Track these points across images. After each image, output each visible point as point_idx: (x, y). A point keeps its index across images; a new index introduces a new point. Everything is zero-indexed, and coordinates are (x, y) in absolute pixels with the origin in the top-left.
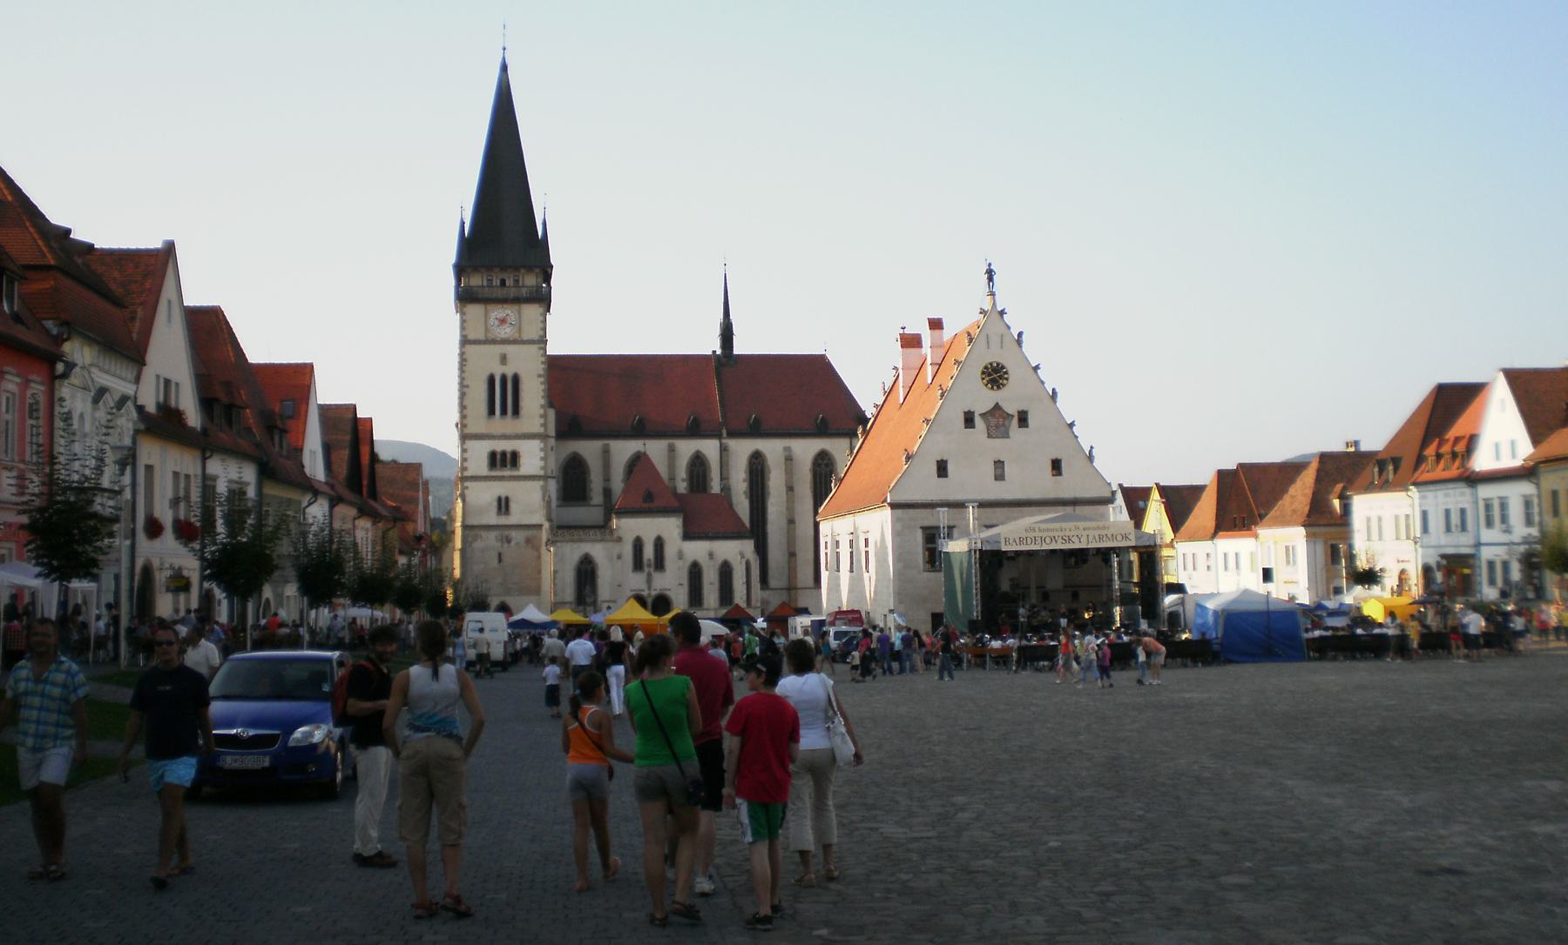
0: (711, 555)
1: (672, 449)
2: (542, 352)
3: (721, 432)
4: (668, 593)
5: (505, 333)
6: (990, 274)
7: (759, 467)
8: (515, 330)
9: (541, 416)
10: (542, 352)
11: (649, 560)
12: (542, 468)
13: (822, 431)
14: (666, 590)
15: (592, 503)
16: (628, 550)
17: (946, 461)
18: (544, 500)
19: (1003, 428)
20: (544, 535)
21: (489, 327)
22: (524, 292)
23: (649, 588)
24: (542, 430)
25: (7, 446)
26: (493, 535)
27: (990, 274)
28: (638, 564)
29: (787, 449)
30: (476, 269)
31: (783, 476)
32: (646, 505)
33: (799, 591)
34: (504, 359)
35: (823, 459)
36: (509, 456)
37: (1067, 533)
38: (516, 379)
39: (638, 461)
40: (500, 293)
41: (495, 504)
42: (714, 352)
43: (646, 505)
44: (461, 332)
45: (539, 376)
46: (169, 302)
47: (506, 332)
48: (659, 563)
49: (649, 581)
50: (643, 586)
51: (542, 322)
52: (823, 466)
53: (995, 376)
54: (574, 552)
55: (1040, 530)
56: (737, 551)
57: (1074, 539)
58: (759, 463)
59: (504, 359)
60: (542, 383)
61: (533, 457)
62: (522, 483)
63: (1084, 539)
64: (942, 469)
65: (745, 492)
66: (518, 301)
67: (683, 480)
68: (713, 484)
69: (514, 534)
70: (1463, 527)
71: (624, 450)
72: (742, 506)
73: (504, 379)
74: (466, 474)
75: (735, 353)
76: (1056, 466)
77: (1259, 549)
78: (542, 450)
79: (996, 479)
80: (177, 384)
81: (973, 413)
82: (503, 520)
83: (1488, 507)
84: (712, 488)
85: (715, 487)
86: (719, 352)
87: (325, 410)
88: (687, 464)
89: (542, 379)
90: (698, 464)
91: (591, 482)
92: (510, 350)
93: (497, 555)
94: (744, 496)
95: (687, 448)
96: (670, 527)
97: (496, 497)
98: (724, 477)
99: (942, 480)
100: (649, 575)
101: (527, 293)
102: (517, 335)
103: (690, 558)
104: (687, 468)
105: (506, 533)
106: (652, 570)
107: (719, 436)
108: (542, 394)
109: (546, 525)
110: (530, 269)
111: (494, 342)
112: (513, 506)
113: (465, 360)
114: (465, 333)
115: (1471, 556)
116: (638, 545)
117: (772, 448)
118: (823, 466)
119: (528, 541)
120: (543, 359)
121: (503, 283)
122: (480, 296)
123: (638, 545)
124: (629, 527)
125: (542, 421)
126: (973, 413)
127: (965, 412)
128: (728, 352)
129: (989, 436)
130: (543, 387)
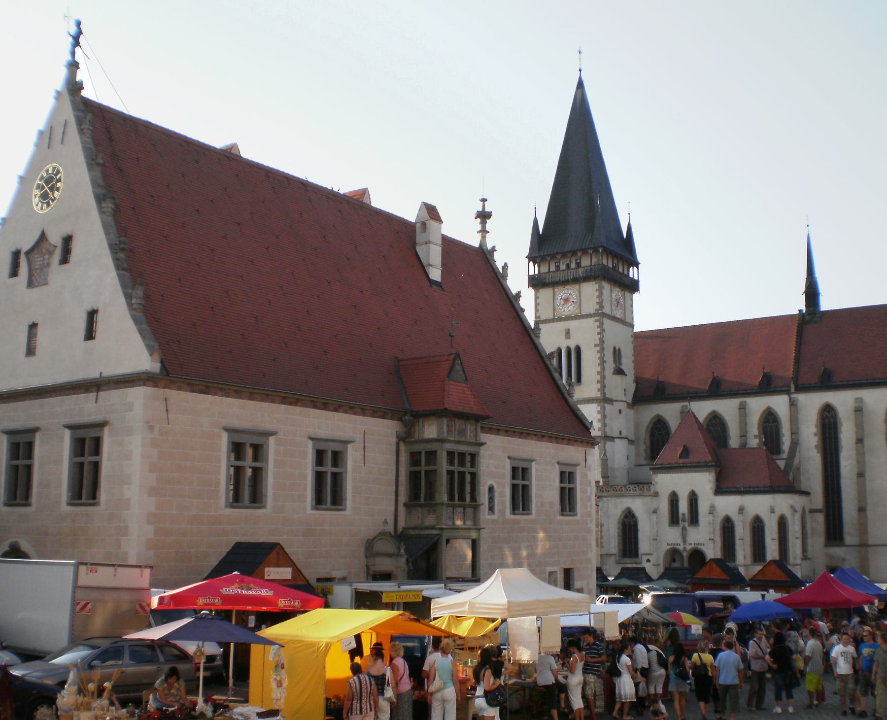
1: (743, 407)
3: (789, 386)
4: (701, 547)
8: (576, 307)
10: (598, 324)
11: (684, 514)
14: (701, 544)
21: (556, 305)
23: (685, 541)
24: (599, 395)
28: (674, 519)
29: (859, 400)
31: (854, 429)
32: (681, 461)
33: (870, 549)
34: (568, 333)
38: (578, 350)
40: (561, 276)
42: (800, 311)
44: (535, 314)
45: (596, 345)
47: (569, 309)
48: (694, 519)
50: (679, 540)
51: (597, 297)
54: (616, 507)
58: (832, 417)
59: (568, 333)
60: (598, 352)
65: (816, 447)
66: (576, 280)
67: (755, 437)
73: (569, 350)
78: (599, 412)
88: (760, 421)
89: (598, 348)
90: (770, 419)
92: (572, 325)
94: (815, 450)
95: (757, 405)
98: (795, 433)
100: (684, 529)
103: (721, 513)
104: (759, 425)
106: (686, 524)
107: (788, 392)
110: (584, 252)
111: (560, 319)
116: (674, 500)
121: (568, 266)
122: (547, 281)
123: (674, 500)
125: (599, 386)
128: (811, 309)
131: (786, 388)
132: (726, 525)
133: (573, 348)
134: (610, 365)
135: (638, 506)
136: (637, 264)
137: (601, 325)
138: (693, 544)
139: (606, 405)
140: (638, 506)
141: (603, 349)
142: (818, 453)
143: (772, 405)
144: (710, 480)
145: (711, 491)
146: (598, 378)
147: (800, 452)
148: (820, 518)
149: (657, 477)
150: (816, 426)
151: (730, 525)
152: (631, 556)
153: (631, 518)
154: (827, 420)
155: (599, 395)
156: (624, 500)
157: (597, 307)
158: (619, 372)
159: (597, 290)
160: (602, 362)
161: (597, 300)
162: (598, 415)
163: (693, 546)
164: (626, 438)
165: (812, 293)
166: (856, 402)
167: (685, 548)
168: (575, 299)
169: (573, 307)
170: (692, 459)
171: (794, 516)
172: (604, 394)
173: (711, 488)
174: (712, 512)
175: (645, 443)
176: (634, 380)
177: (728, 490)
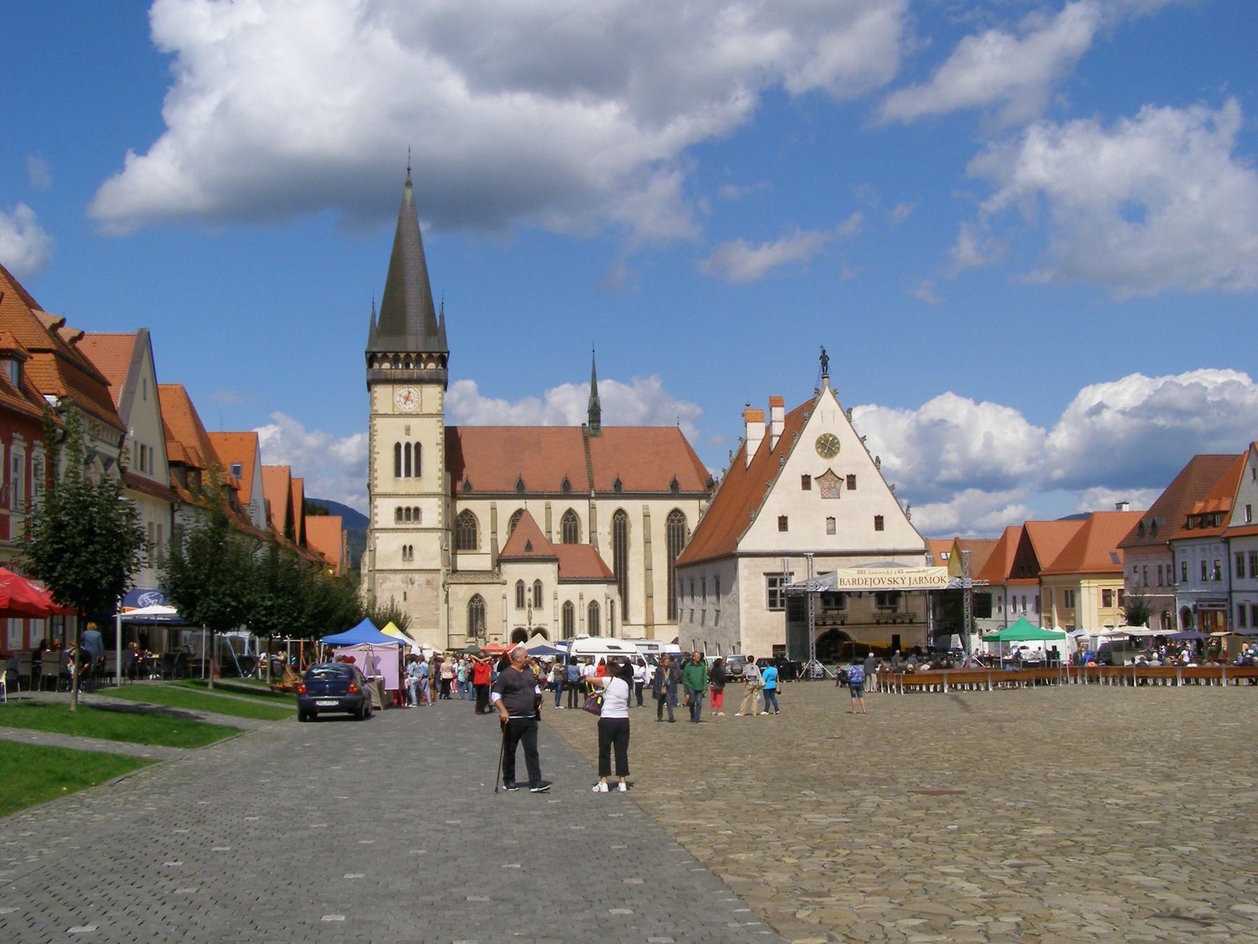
0: (581, 597)
2: (440, 424)
4: (544, 627)
6: (824, 360)
7: (622, 522)
10: (440, 424)
12: (440, 522)
13: (675, 491)
15: (482, 551)
16: (511, 591)
17: (786, 518)
18: (441, 548)
19: (835, 490)
20: (441, 578)
23: (530, 624)
25: (402, 495)
26: (399, 577)
27: (824, 360)
28: (520, 603)
29: (646, 508)
30: (385, 358)
34: (408, 430)
35: (676, 516)
36: (412, 511)
37: (893, 576)
38: (418, 446)
39: (520, 512)
40: (405, 374)
41: (401, 552)
43: (527, 554)
45: (438, 444)
46: (145, 380)
47: (409, 407)
48: (538, 602)
49: (530, 619)
51: (440, 399)
52: (676, 522)
53: (828, 446)
55: (870, 573)
56: (600, 592)
57: (899, 581)
59: (408, 430)
60: (440, 450)
61: (432, 513)
62: (423, 534)
63: (907, 581)
64: (783, 523)
65: (610, 543)
66: (420, 381)
67: (558, 533)
68: (583, 536)
69: (416, 576)
70: (1218, 577)
71: (508, 508)
72: (608, 557)
73: (408, 446)
74: (377, 526)
75: (603, 424)
76: (879, 523)
77: (1042, 592)
78: (439, 506)
79: (829, 533)
80: (151, 449)
81: (809, 477)
82: (407, 566)
83: (1240, 560)
84: (582, 539)
85: (585, 539)
86: (587, 425)
89: (440, 447)
90: (570, 516)
91: (481, 534)
93: (403, 594)
95: (560, 507)
96: (547, 573)
97: (402, 547)
98: (593, 532)
99: (783, 533)
100: (530, 612)
102: (419, 410)
105: (410, 575)
107: (588, 497)
108: (440, 460)
109: (444, 570)
111: (401, 415)
112: (415, 552)
113: (376, 431)
114: (375, 408)
115: (1226, 600)
117: (633, 508)
118: (676, 522)
119: (428, 583)
120: (441, 430)
122: (388, 377)
123: (520, 587)
124: (513, 572)
126: (809, 477)
127: (803, 477)
128: (595, 424)
129: (823, 498)
130: (441, 453)
143: (574, 508)
155: (440, 490)
157: (440, 408)
161: (440, 402)
163: (537, 626)
165: (594, 412)
166: (644, 509)
170: (535, 552)
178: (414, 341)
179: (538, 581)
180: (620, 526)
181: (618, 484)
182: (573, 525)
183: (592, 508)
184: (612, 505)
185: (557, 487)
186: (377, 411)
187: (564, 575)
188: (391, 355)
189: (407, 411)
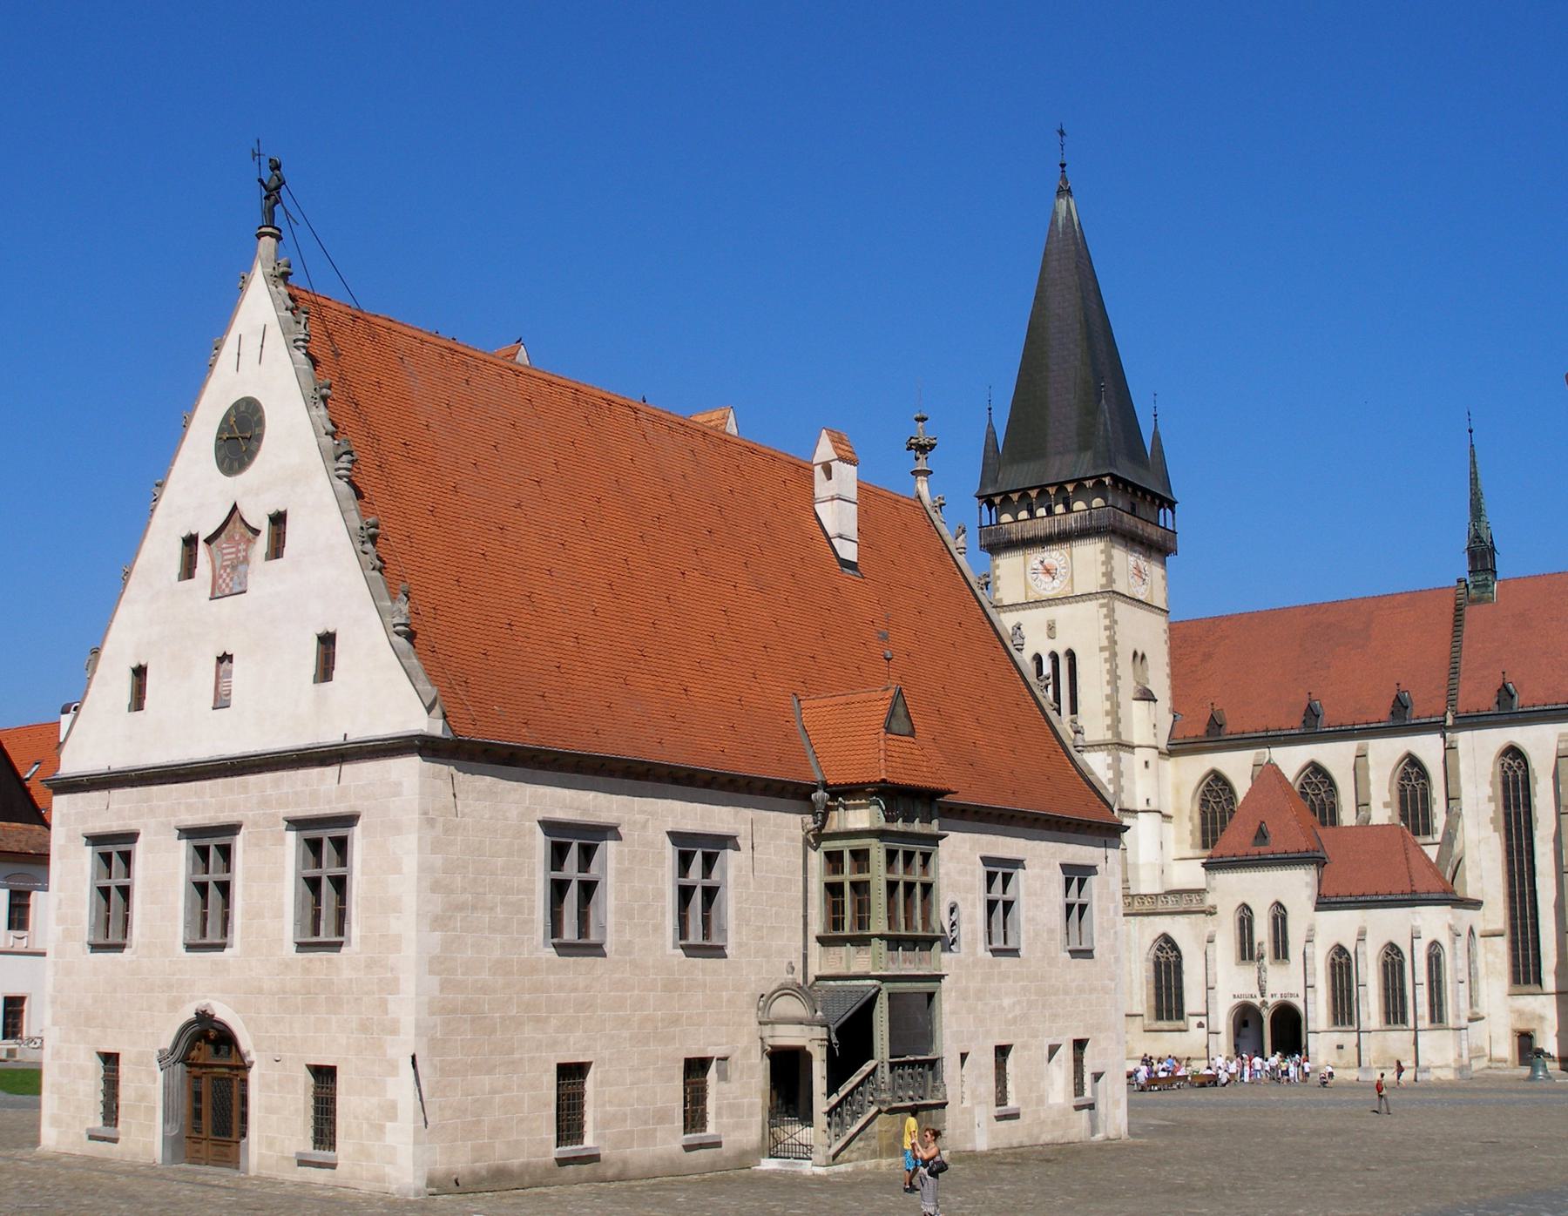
1: (1362, 755)
2: (1104, 611)
5: (1054, 588)
7: (1520, 773)
9: (1107, 713)
10: (1104, 611)
14: (1292, 995)
22: (1071, 521)
24: (1108, 736)
28: (1247, 951)
34: (1051, 628)
38: (1071, 655)
43: (1255, 850)
45: (1102, 649)
48: (1281, 951)
50: (1255, 990)
51: (1103, 563)
59: (1051, 628)
60: (1106, 660)
65: (1493, 821)
67: (1386, 805)
73: (1054, 657)
87: (1367, 744)
89: (1106, 654)
92: (1059, 613)
94: (1491, 827)
95: (1386, 753)
101: (1076, 522)
107: (1439, 727)
114: (998, 596)
121: (1050, 512)
125: (1108, 721)
131: (1439, 719)
132: (1337, 960)
133: (1061, 653)
134: (1128, 686)
135: (1181, 930)
136: (1172, 504)
137: (1111, 614)
138: (1279, 995)
139: (1122, 754)
140: (1181, 930)
141: (1114, 655)
142: (1495, 831)
144: (1307, 883)
145: (1310, 902)
146: (1107, 706)
147: (1463, 830)
148: (1502, 945)
149: (1214, 879)
150: (1492, 784)
151: (1343, 960)
152: (1170, 1018)
153: (1168, 950)
154: (1510, 774)
156: (1157, 919)
157: (1103, 581)
158: (1147, 696)
159: (1102, 552)
160: (1114, 679)
161: (1103, 569)
162: (1107, 772)
163: (1278, 999)
164: (1160, 812)
165: (1482, 556)
167: (1264, 1001)
168: (1064, 568)
169: (1061, 582)
170: (1276, 845)
171: (1454, 943)
172: (1117, 734)
173: (1309, 898)
174: (1311, 939)
175: (1191, 819)
176: (1169, 709)
177: (1339, 899)
178: (1059, 467)
179: (1279, 905)
180: (1516, 783)
181: (1505, 694)
182: (1418, 788)
183: (1450, 748)
184: (1497, 738)
185: (1382, 712)
186: (1001, 600)
187: (1329, 892)
188: (1015, 497)
189: (1050, 594)
